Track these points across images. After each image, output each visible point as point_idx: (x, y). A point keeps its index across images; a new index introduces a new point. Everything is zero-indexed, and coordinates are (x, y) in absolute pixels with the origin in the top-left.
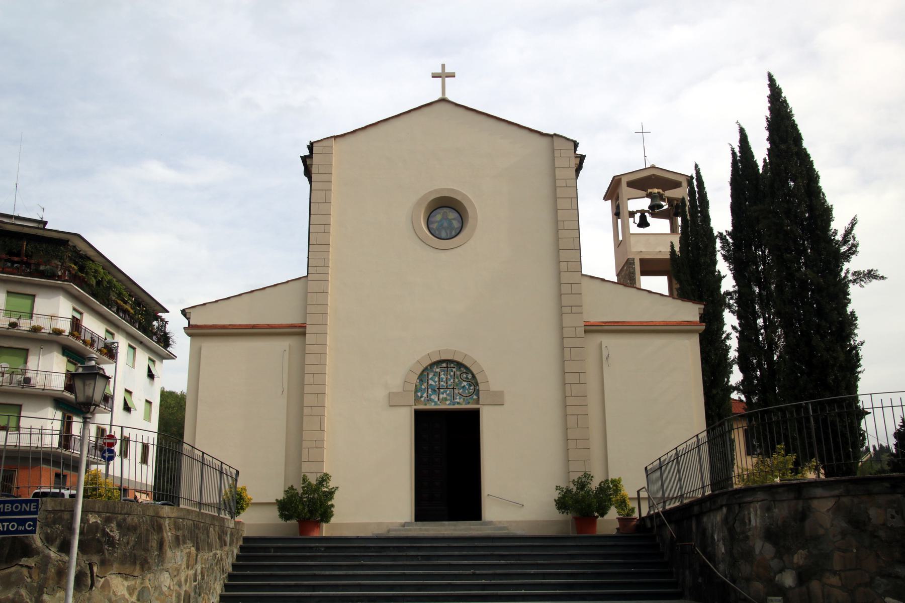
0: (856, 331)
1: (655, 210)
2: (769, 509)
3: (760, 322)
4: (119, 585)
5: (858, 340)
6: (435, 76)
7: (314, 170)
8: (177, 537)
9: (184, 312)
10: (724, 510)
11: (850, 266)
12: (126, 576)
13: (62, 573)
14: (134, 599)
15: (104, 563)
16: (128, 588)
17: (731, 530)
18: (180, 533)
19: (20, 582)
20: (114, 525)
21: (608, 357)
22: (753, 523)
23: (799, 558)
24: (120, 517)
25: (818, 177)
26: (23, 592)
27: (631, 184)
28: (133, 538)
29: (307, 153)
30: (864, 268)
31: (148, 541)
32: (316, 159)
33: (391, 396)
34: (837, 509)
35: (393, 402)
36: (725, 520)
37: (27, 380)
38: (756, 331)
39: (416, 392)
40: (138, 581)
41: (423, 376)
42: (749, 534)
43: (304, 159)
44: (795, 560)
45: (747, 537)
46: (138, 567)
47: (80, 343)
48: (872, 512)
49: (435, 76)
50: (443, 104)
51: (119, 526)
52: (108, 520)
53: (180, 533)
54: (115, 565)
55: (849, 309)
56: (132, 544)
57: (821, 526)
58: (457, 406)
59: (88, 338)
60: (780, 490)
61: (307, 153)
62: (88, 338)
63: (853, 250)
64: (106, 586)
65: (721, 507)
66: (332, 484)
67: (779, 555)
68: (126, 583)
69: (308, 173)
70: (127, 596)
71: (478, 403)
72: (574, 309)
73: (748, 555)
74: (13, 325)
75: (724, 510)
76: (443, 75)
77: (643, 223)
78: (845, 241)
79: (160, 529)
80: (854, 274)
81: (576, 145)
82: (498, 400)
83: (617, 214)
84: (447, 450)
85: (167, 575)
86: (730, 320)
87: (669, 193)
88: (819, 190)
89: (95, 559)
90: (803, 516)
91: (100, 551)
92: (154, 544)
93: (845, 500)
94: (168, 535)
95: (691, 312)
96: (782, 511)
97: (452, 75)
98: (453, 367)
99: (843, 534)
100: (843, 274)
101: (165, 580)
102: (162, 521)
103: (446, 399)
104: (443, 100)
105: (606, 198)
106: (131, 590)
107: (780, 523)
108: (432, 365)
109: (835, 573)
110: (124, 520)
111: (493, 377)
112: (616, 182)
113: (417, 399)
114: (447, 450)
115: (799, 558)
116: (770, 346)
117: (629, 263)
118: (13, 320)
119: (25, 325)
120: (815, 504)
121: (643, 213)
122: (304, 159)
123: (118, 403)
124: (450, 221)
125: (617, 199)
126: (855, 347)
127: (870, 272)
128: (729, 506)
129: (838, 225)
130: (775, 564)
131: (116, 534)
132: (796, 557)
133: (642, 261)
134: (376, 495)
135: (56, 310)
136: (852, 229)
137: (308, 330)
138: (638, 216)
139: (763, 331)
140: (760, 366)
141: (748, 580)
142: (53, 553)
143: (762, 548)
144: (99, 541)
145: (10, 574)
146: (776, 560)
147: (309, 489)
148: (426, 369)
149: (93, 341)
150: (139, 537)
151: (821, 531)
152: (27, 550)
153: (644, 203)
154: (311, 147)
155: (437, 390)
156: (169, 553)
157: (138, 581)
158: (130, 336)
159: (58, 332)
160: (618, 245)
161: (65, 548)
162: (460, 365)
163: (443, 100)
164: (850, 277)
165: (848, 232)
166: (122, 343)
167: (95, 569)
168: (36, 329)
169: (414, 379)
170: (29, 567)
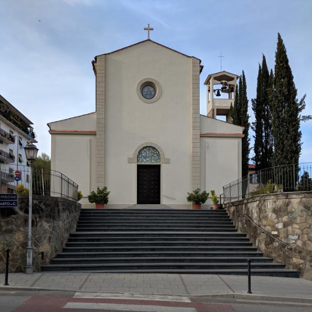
0: (301, 139)
2: (275, 202)
3: (264, 134)
4: (46, 225)
8: (64, 209)
10: (258, 202)
11: (301, 114)
12: (48, 222)
13: (26, 221)
14: (51, 230)
15: (40, 217)
16: (49, 226)
17: (260, 209)
18: (64, 207)
19: (12, 223)
20: (42, 204)
21: (208, 147)
22: (269, 207)
23: (285, 219)
24: (44, 201)
25: (293, 77)
26: (14, 227)
27: (215, 78)
28: (49, 208)
30: (307, 115)
31: (54, 210)
33: (129, 159)
34: (300, 202)
35: (130, 161)
36: (258, 206)
38: (262, 137)
40: (52, 224)
42: (267, 210)
44: (283, 219)
45: (266, 212)
46: (52, 219)
51: (44, 204)
52: (40, 202)
53: (64, 207)
54: (44, 218)
56: (49, 210)
57: (294, 208)
60: (280, 195)
63: (303, 107)
64: (41, 225)
65: (257, 201)
66: (108, 190)
67: (277, 218)
68: (48, 224)
70: (49, 229)
71: (160, 162)
72: (194, 128)
73: (266, 217)
75: (258, 202)
77: (218, 95)
78: (301, 104)
79: (58, 206)
82: (168, 161)
85: (61, 222)
86: (252, 133)
87: (229, 83)
88: (293, 83)
89: (37, 216)
90: (288, 205)
91: (39, 213)
92: (56, 211)
94: (61, 208)
95: (239, 130)
99: (302, 211)
100: (298, 117)
101: (61, 223)
102: (58, 203)
106: (50, 227)
107: (279, 207)
109: (297, 224)
110: (46, 202)
111: (166, 152)
112: (210, 77)
115: (285, 219)
116: (266, 144)
123: (16, 159)
124: (151, 91)
127: (309, 116)
128: (260, 201)
129: (299, 98)
130: (276, 221)
131: (43, 207)
132: (284, 218)
133: (217, 109)
134: (124, 194)
136: (304, 99)
137: (97, 133)
138: (216, 91)
139: (264, 138)
141: (265, 226)
142: (21, 213)
143: (272, 216)
144: (38, 209)
145: (8, 220)
146: (276, 219)
147: (100, 192)
148: (141, 149)
150: (51, 208)
151: (294, 210)
152: (15, 213)
153: (220, 87)
156: (61, 214)
157: (52, 224)
161: (27, 212)
164: (301, 118)
165: (302, 100)
167: (38, 220)
170: (14, 218)
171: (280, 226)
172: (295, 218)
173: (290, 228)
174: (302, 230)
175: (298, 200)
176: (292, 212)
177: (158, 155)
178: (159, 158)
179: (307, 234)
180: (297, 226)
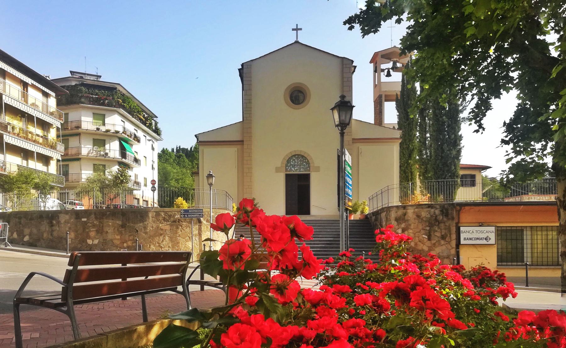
1: (395, 68)
5: (462, 145)
6: (293, 30)
7: (244, 75)
9: (196, 136)
23: (403, 225)
27: (383, 56)
29: (241, 67)
32: (245, 70)
37: (107, 154)
38: (426, 138)
39: (286, 167)
41: (288, 161)
43: (239, 70)
47: (126, 136)
48: (423, 213)
49: (293, 30)
50: (297, 45)
55: (460, 133)
58: (301, 173)
59: (129, 134)
61: (241, 67)
62: (129, 134)
67: (398, 225)
69: (241, 75)
74: (98, 129)
76: (297, 29)
77: (389, 75)
80: (463, 118)
81: (352, 62)
83: (375, 71)
84: (298, 191)
90: (405, 214)
93: (416, 210)
96: (400, 212)
97: (301, 29)
98: (301, 158)
99: (415, 219)
103: (297, 170)
104: (297, 42)
105: (371, 62)
108: (292, 157)
112: (376, 54)
113: (286, 170)
114: (298, 191)
115: (403, 225)
117: (380, 97)
118: (98, 127)
119: (103, 129)
120: (408, 211)
121: (388, 69)
122: (239, 70)
125: (376, 63)
126: (461, 148)
130: (397, 227)
133: (386, 96)
135: (115, 122)
138: (386, 71)
140: (426, 153)
149: (131, 135)
153: (390, 65)
154: (242, 65)
155: (294, 166)
158: (144, 131)
159: (117, 132)
160: (375, 86)
162: (303, 156)
163: (297, 42)
166: (140, 134)
168: (108, 131)
169: (285, 162)
171: (400, 231)
172: (410, 225)
173: (406, 232)
174: (415, 234)
175: (412, 211)
176: (408, 220)
177: (308, 163)
178: (309, 167)
179: (418, 237)
180: (411, 231)
